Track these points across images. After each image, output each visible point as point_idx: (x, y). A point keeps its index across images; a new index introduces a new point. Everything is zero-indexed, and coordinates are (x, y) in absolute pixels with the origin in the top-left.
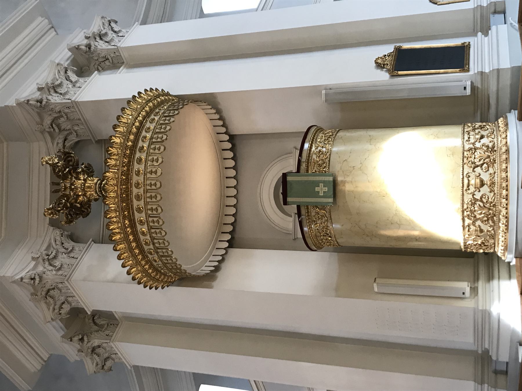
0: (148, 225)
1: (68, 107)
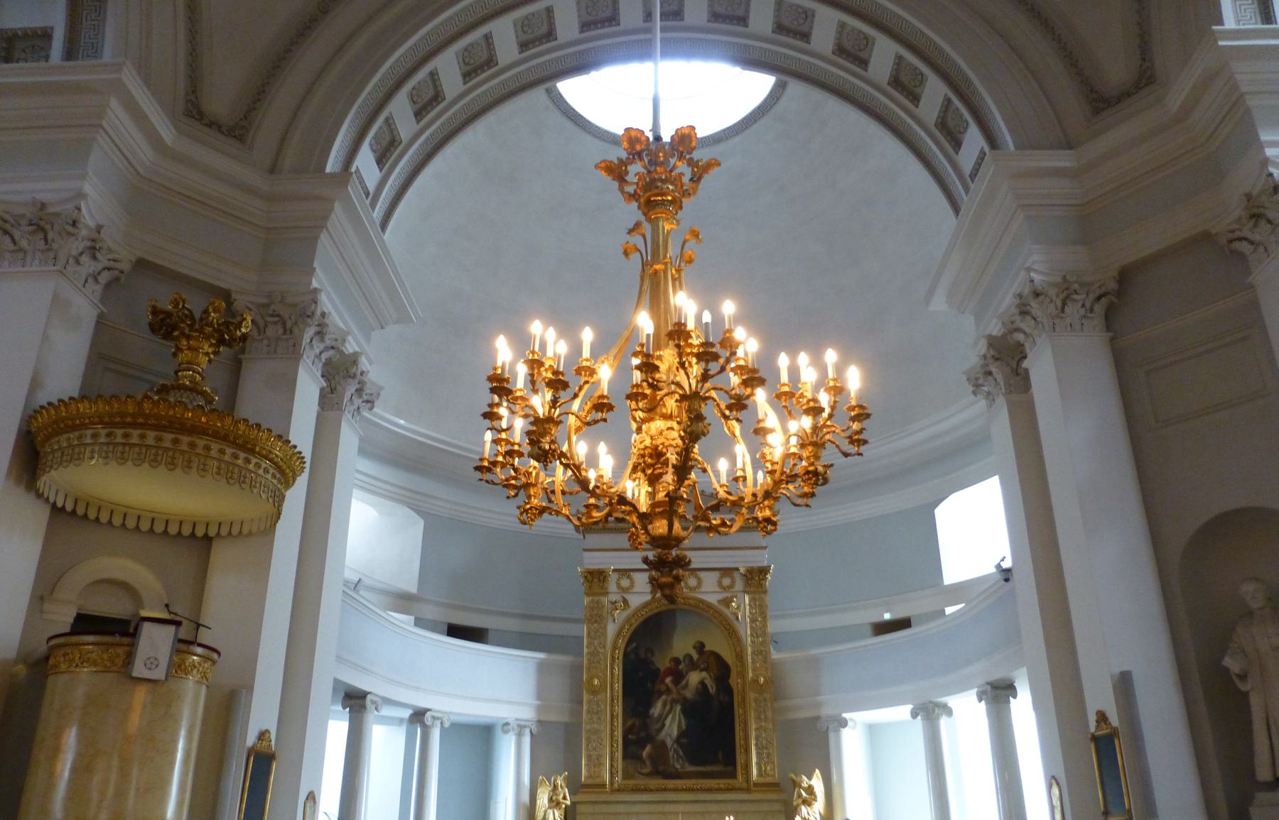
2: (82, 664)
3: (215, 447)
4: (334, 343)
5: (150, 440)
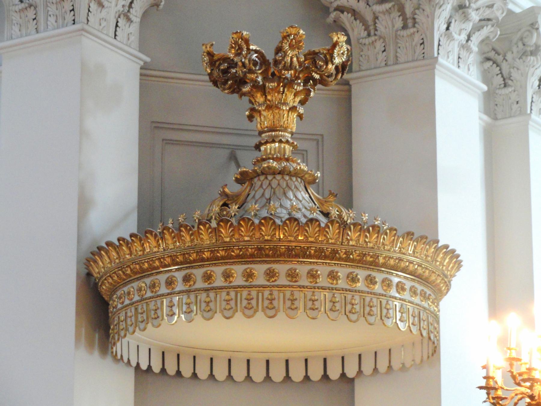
0: (244, 287)
3: (323, 270)
4: (487, 13)
5: (238, 280)
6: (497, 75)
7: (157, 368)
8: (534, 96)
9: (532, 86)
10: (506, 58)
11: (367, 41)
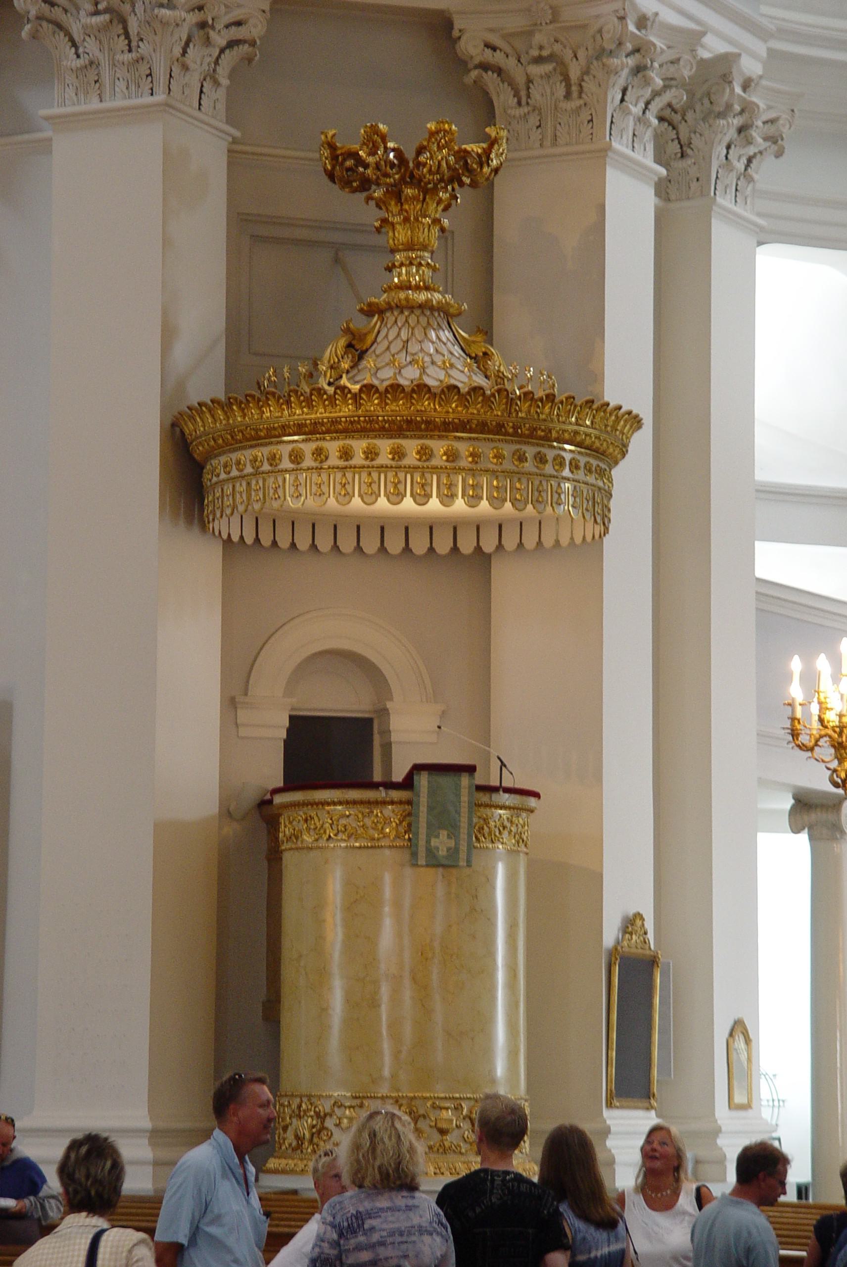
1: (592, 120)
2: (336, 835)
6: (672, 140)
7: (249, 540)
8: (720, 171)
9: (719, 156)
10: (686, 118)
11: (518, 112)
